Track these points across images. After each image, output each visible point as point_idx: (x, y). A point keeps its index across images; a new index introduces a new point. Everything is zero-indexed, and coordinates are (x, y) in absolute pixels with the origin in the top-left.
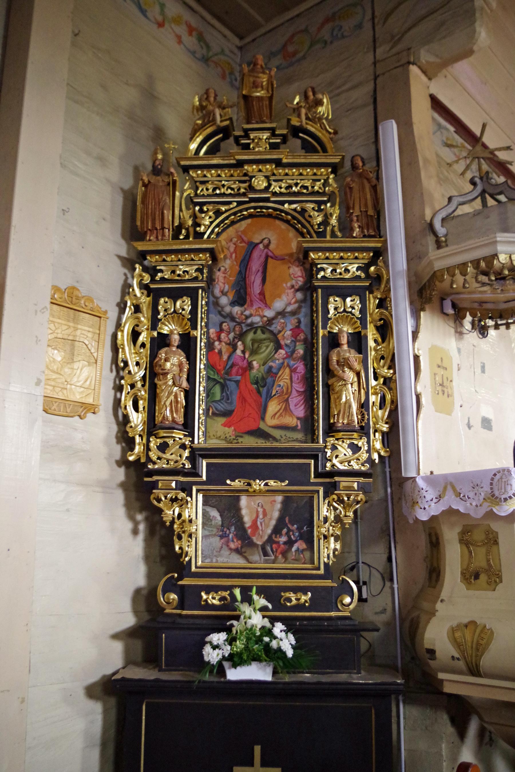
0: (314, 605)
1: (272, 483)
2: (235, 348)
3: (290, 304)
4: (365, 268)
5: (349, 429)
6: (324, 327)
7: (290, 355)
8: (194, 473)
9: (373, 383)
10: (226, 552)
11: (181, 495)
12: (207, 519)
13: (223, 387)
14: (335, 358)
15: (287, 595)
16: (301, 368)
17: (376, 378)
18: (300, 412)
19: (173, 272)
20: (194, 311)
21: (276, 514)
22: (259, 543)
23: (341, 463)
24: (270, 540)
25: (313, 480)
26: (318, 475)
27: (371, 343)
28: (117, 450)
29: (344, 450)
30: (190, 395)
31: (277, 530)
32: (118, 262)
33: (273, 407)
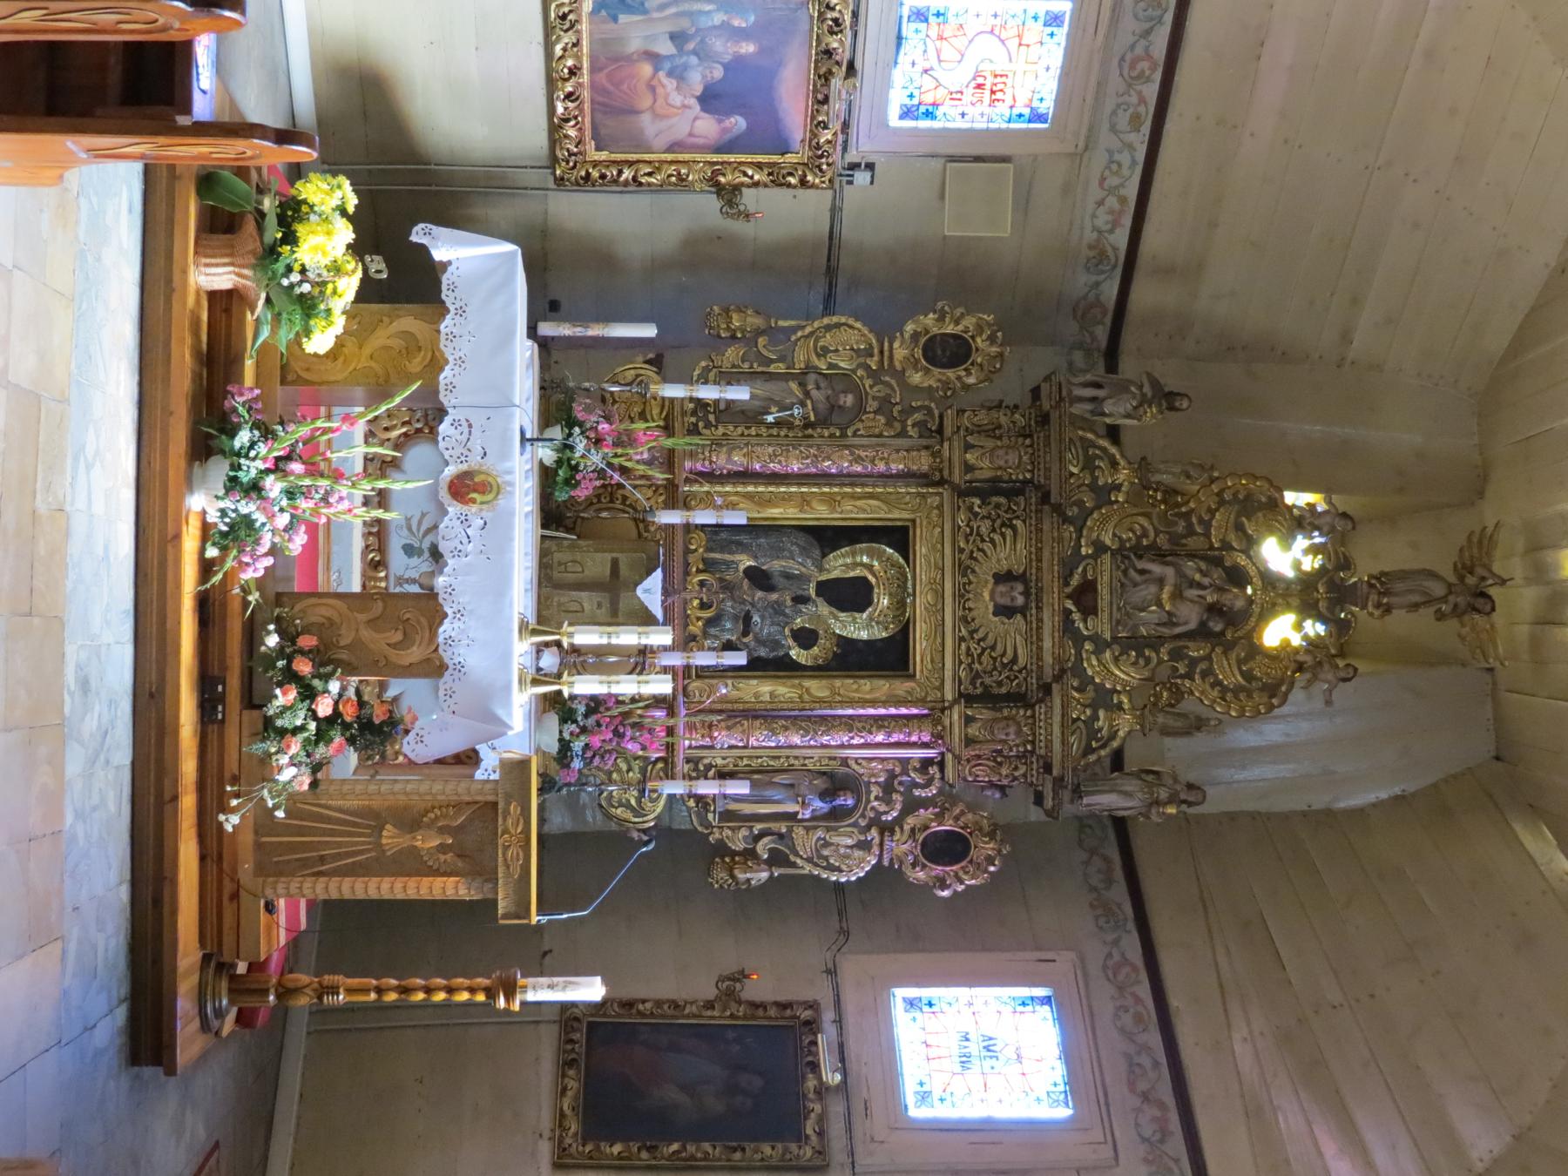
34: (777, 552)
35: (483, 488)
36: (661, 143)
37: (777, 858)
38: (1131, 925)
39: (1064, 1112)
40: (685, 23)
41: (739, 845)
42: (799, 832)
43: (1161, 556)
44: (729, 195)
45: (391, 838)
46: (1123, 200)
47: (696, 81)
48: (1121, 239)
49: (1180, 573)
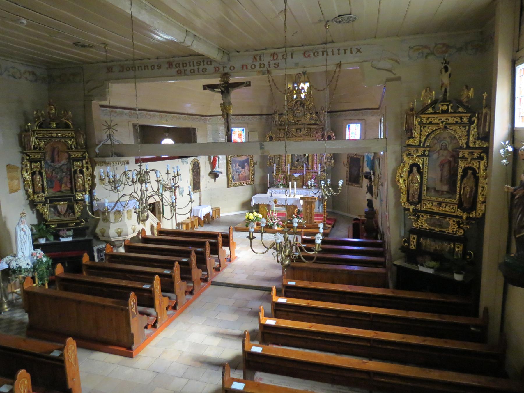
0: (75, 225)
1: (64, 202)
2: (52, 172)
3: (65, 162)
4: (82, 155)
5: (80, 191)
6: (73, 168)
7: (66, 174)
8: (46, 201)
9: (86, 180)
10: (55, 216)
11: (44, 206)
12: (50, 211)
13: (51, 182)
14: (76, 176)
15: (69, 224)
16: (69, 177)
17: (86, 179)
18: (69, 186)
19: (34, 157)
20: (41, 166)
21: (66, 208)
22: (63, 214)
23: (79, 197)
24: (65, 213)
25: (73, 201)
26: (74, 200)
27: (85, 171)
28: (26, 197)
29: (80, 195)
30: (43, 185)
31: (66, 211)
32: (19, 153)
33: (63, 186)
34: (295, 158)
35: (275, 200)
36: (249, 173)
37: (331, 159)
38: (341, 113)
39: (359, 125)
40: (235, 172)
41: (329, 163)
42: (327, 156)
43: (294, 113)
44: (254, 164)
45: (308, 211)
46: (253, 117)
47: (241, 169)
48: (258, 116)
49: (296, 110)
